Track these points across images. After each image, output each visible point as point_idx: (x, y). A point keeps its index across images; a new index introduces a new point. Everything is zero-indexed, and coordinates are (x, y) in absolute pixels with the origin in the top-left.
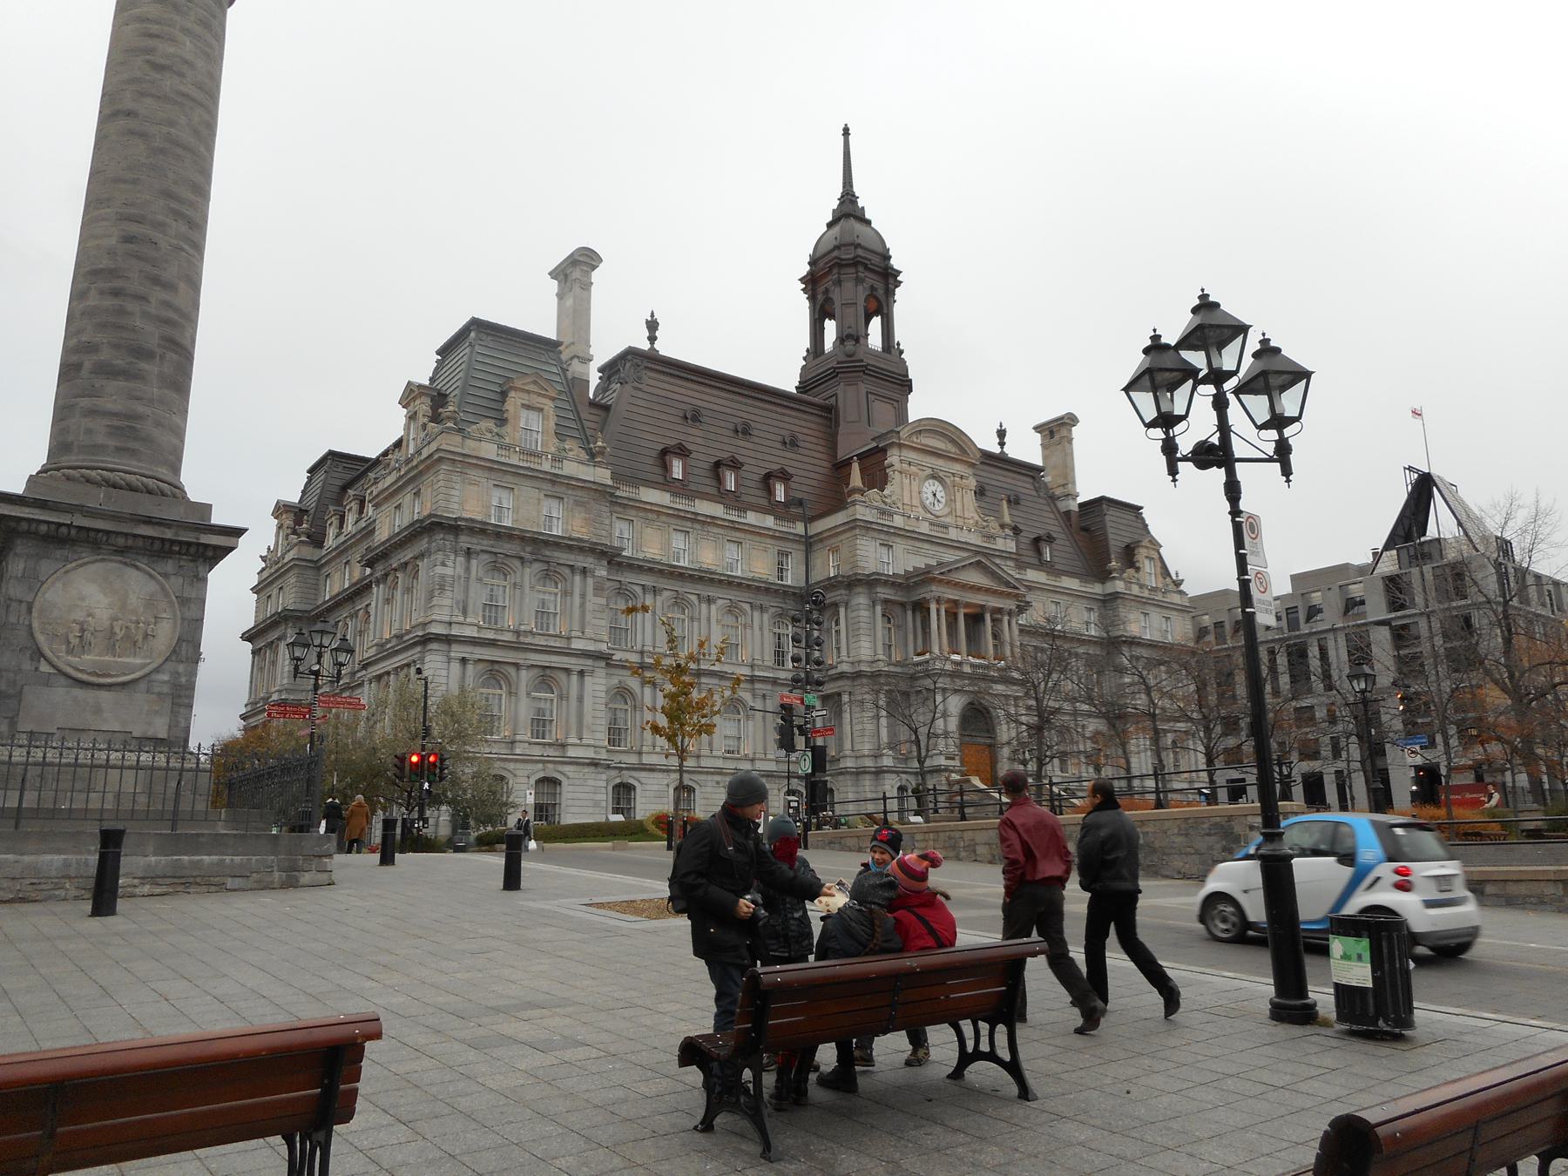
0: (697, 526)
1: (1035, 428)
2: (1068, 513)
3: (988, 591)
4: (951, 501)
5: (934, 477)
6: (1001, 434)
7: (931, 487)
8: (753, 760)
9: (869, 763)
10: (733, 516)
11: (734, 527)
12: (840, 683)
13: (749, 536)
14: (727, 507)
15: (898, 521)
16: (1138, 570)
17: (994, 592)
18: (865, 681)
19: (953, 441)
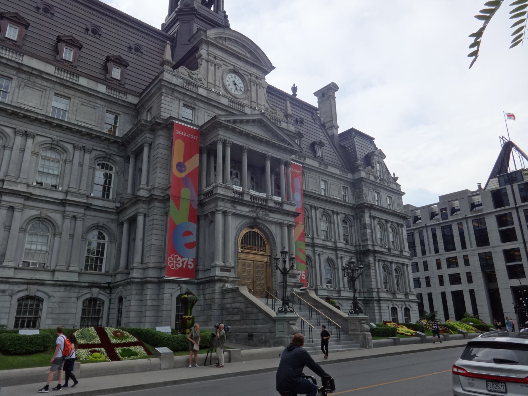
0: (23, 76)
1: (316, 94)
2: (333, 136)
3: (267, 143)
4: (247, 90)
5: (235, 72)
6: (294, 89)
7: (230, 78)
8: (53, 271)
9: (152, 273)
10: (65, 76)
11: (63, 84)
12: (137, 206)
13: (79, 95)
14: (58, 68)
15: (201, 91)
16: (373, 167)
17: (273, 146)
18: (157, 204)
19: (250, 52)
